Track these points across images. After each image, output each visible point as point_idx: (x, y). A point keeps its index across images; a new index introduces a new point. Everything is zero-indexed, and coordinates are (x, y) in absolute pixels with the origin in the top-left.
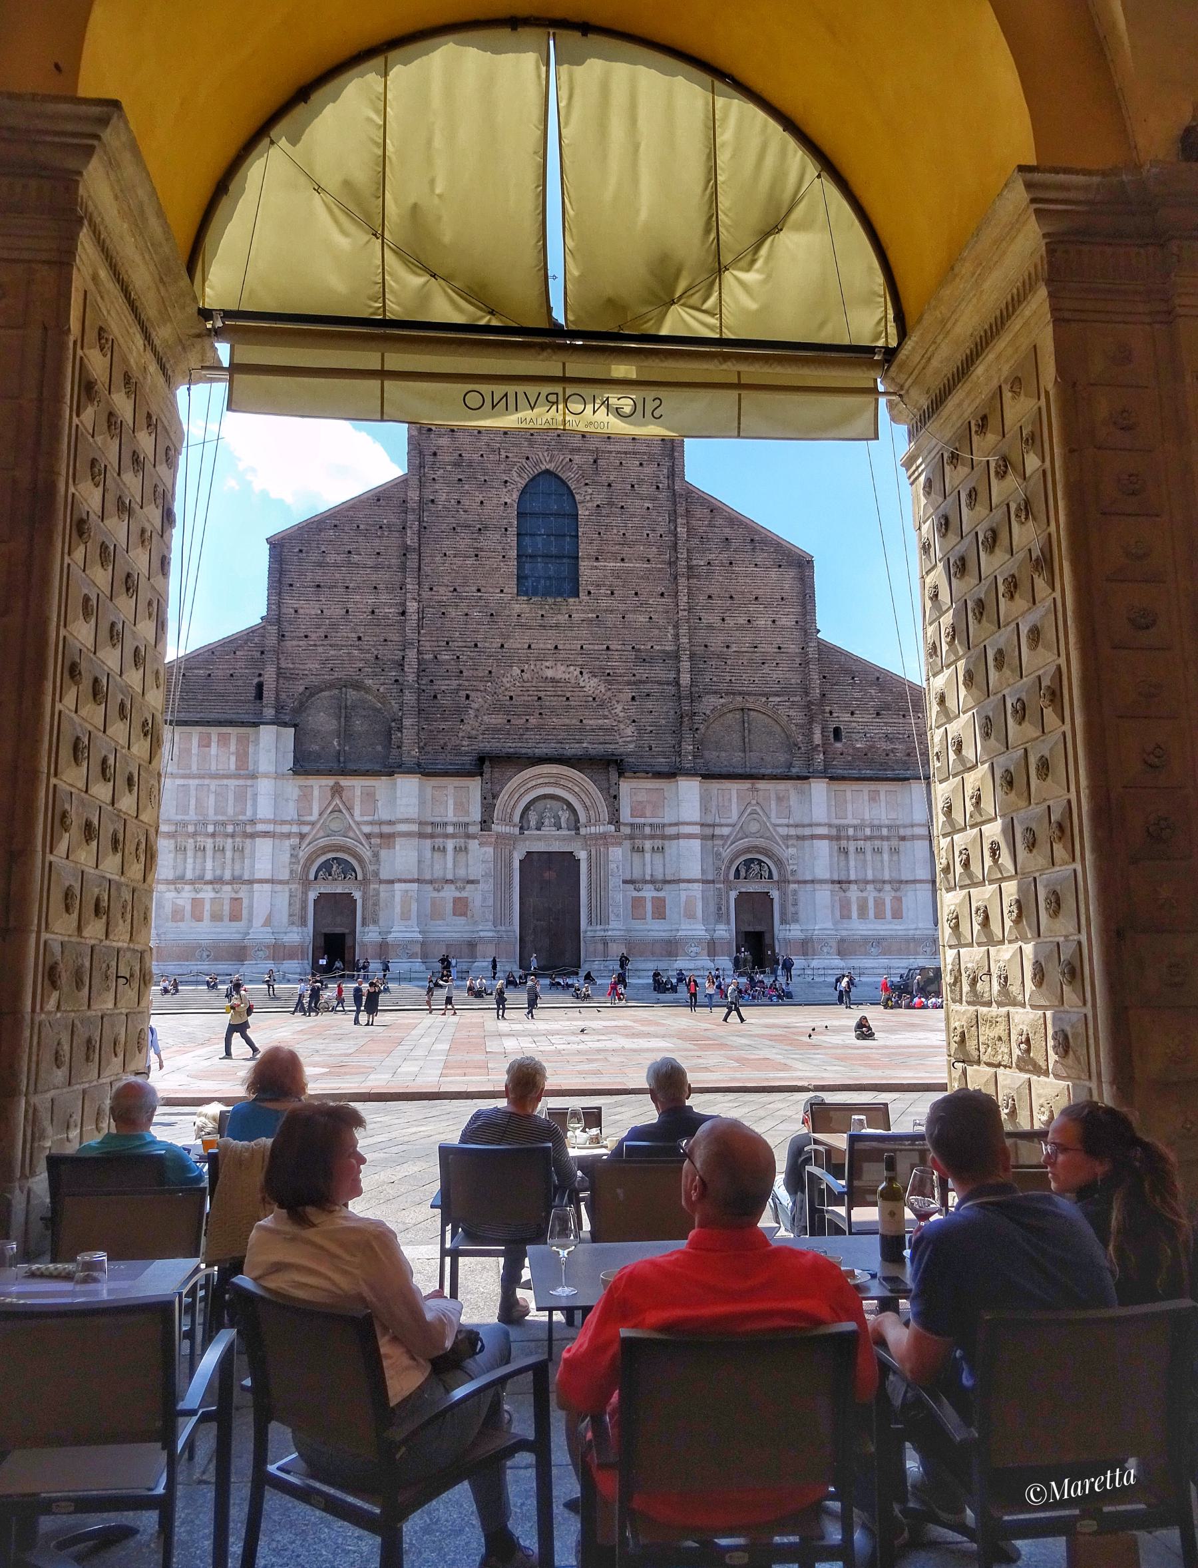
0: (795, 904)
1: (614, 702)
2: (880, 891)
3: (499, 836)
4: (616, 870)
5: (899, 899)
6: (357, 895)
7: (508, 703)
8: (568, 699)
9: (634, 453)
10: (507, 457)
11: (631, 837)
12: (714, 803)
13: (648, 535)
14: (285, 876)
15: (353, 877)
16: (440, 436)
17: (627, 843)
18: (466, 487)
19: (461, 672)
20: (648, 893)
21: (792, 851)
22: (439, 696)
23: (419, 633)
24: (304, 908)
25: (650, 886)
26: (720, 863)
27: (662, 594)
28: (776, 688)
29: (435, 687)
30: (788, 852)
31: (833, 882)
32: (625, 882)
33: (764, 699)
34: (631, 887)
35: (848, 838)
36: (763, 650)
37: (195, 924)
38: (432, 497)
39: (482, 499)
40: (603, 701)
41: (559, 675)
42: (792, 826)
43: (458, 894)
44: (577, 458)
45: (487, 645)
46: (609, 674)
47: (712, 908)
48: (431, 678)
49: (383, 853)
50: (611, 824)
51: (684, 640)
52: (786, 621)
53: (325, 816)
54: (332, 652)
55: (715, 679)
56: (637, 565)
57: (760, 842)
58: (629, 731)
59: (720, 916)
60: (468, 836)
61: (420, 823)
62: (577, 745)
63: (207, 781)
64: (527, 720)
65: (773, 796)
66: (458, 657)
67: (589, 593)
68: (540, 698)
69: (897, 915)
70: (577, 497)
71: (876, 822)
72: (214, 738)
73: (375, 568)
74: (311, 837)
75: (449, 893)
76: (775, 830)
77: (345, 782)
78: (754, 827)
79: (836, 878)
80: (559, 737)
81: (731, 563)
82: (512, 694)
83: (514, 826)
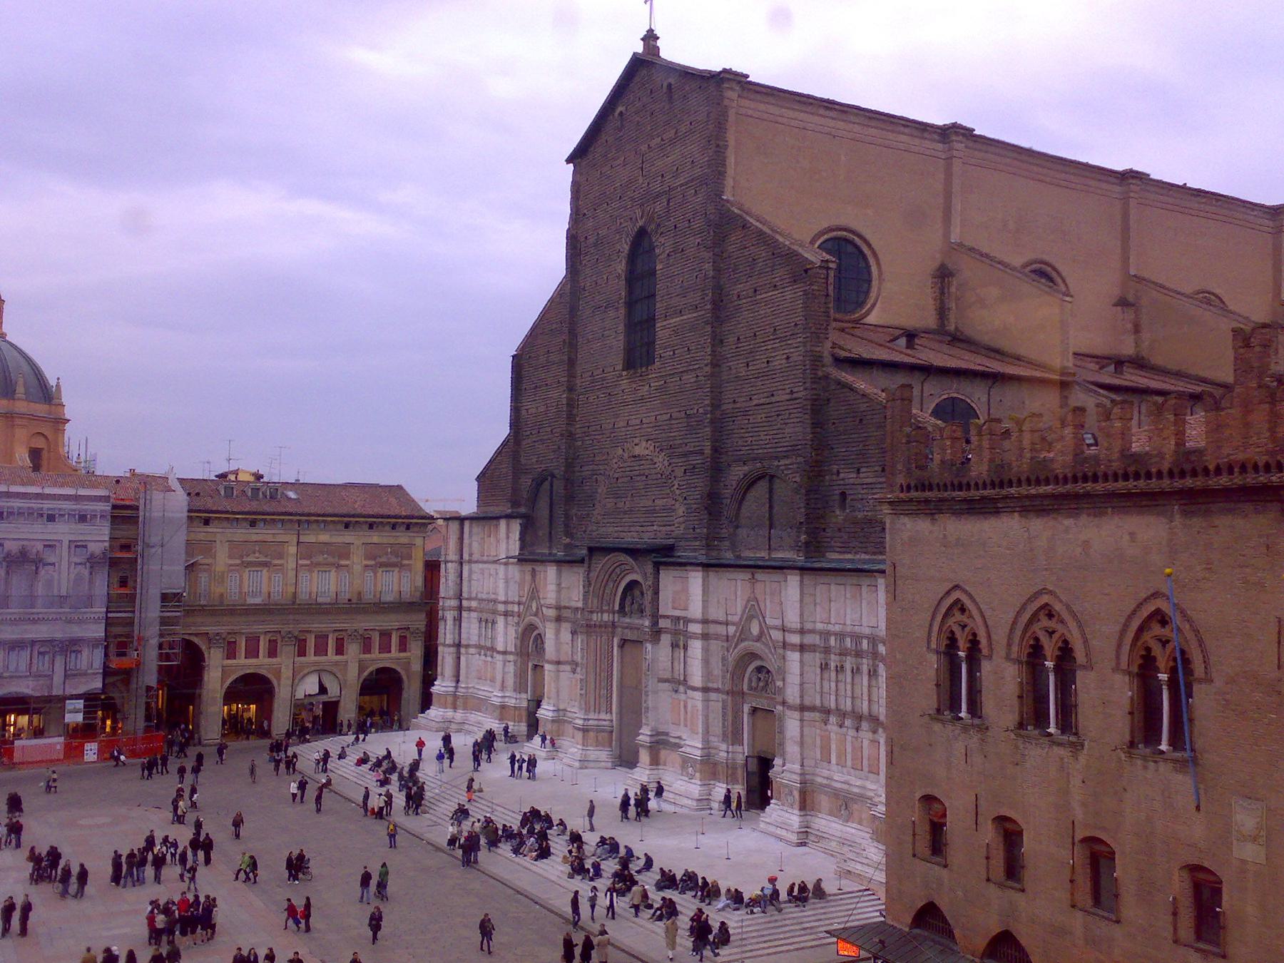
9: (692, 180)
14: (511, 648)
17: (666, 639)
30: (772, 663)
33: (776, 463)
35: (827, 650)
55: (739, 443)
56: (690, 316)
57: (757, 647)
58: (681, 510)
61: (558, 608)
70: (657, 251)
77: (539, 568)
78: (755, 630)
79: (818, 703)
81: (755, 291)
83: (614, 614)
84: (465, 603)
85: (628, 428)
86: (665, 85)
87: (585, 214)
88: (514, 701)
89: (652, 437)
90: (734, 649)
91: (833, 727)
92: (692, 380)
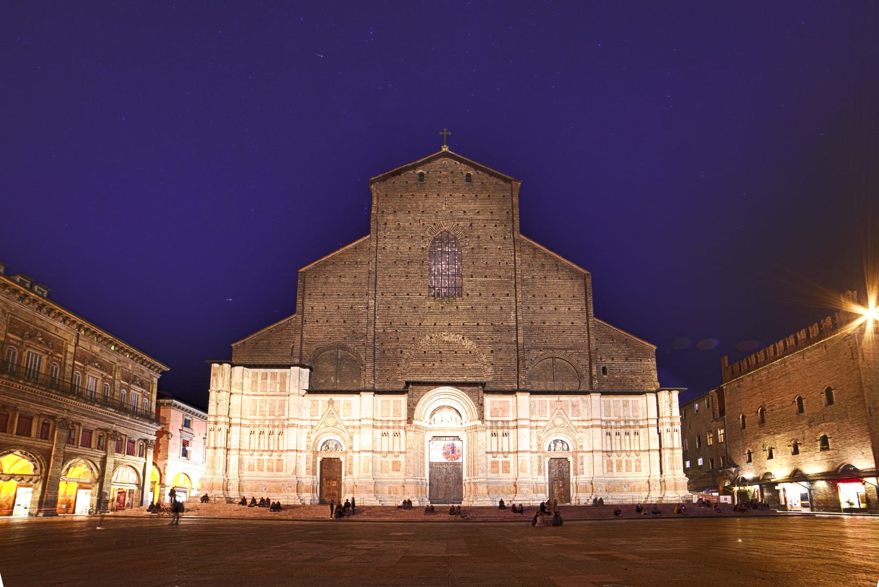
0: (582, 464)
1: (481, 354)
2: (629, 456)
3: (416, 427)
4: (482, 445)
5: (639, 461)
6: (342, 459)
7: (423, 355)
8: (456, 352)
10: (424, 224)
11: (491, 428)
12: (537, 409)
13: (500, 263)
14: (304, 448)
15: (340, 450)
16: (388, 214)
18: (402, 240)
19: (398, 339)
20: (500, 459)
21: (579, 435)
22: (386, 351)
23: (375, 317)
24: (314, 465)
25: (502, 455)
26: (539, 442)
27: (508, 295)
28: (571, 345)
29: (384, 347)
31: (603, 452)
32: (487, 453)
33: (564, 352)
34: (490, 456)
36: (563, 324)
37: (259, 473)
38: (383, 246)
39: (410, 246)
40: (475, 353)
41: (452, 339)
42: (581, 421)
43: (395, 459)
44: (461, 224)
45: (412, 324)
46: (478, 339)
47: (536, 467)
48: (381, 342)
49: (356, 437)
50: (480, 419)
51: (520, 318)
52: (575, 308)
53: (325, 417)
54: (330, 330)
55: (537, 341)
56: (494, 279)
58: (490, 370)
59: (540, 471)
60: (400, 427)
62: (461, 378)
63: (265, 397)
64: (434, 364)
65: (570, 405)
66: (396, 331)
67: (468, 295)
68: (440, 352)
69: (638, 469)
71: (627, 418)
72: (269, 375)
73: (354, 284)
74: (317, 427)
75: (391, 458)
76: (571, 423)
79: (604, 449)
80: (451, 374)
81: (545, 277)
82: (425, 350)
84: (233, 421)
85: (436, 327)
86: (465, 173)
87: (383, 211)
88: (309, 479)
89: (463, 333)
90: (545, 433)
91: (614, 457)
92: (498, 309)
